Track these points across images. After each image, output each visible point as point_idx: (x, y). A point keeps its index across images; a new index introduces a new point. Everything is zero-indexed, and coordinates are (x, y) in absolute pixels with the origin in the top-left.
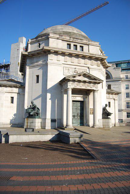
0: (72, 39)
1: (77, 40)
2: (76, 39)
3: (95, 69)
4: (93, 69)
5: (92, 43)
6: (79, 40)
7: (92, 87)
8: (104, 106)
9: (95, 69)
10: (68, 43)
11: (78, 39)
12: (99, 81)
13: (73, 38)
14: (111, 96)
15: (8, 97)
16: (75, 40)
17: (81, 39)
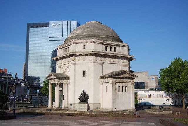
3: (71, 64)
9: (71, 64)
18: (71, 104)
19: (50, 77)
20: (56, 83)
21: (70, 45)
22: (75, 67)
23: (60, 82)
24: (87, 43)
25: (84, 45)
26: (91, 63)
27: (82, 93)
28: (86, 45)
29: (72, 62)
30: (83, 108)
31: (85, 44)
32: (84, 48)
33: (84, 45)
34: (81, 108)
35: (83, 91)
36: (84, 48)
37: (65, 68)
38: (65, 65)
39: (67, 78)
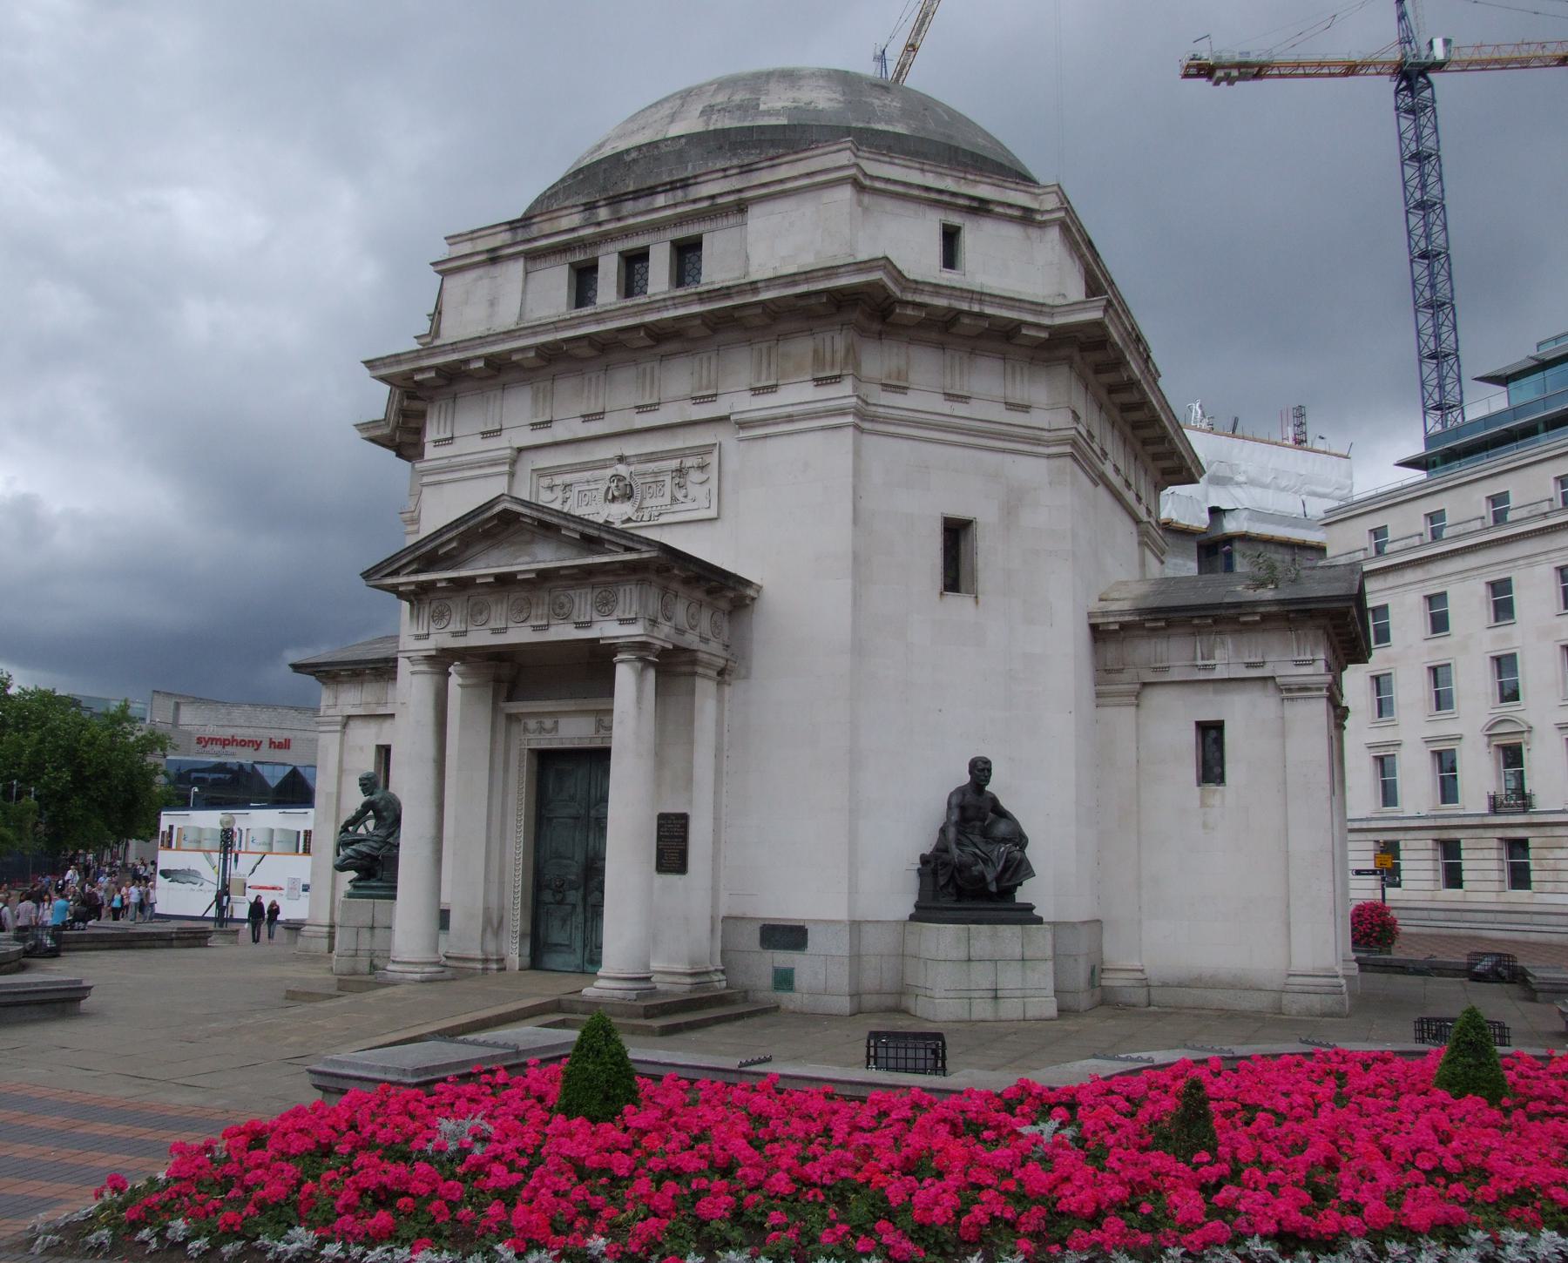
0: (603, 213)
1: (642, 204)
2: (637, 195)
3: (790, 418)
4: (774, 421)
5: (782, 172)
6: (660, 200)
7: (596, 617)
8: (966, 778)
9: (790, 418)
10: (579, 257)
11: (652, 191)
12: (628, 549)
13: (615, 201)
14: (1227, 657)
15: (361, 749)
16: (629, 207)
17: (672, 186)
18: (788, 936)
19: (450, 560)
20: (608, 630)
21: (741, 208)
22: (857, 453)
23: (663, 635)
24: (980, 208)
25: (951, 237)
26: (1038, 441)
27: (961, 791)
28: (977, 238)
29: (798, 394)
30: (1010, 979)
31: (955, 219)
32: (950, 258)
33: (951, 237)
34: (981, 977)
35: (980, 770)
36: (950, 258)
37: (622, 469)
38: (631, 448)
39: (724, 592)
